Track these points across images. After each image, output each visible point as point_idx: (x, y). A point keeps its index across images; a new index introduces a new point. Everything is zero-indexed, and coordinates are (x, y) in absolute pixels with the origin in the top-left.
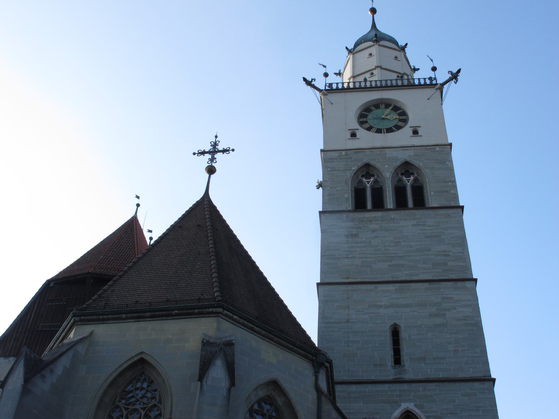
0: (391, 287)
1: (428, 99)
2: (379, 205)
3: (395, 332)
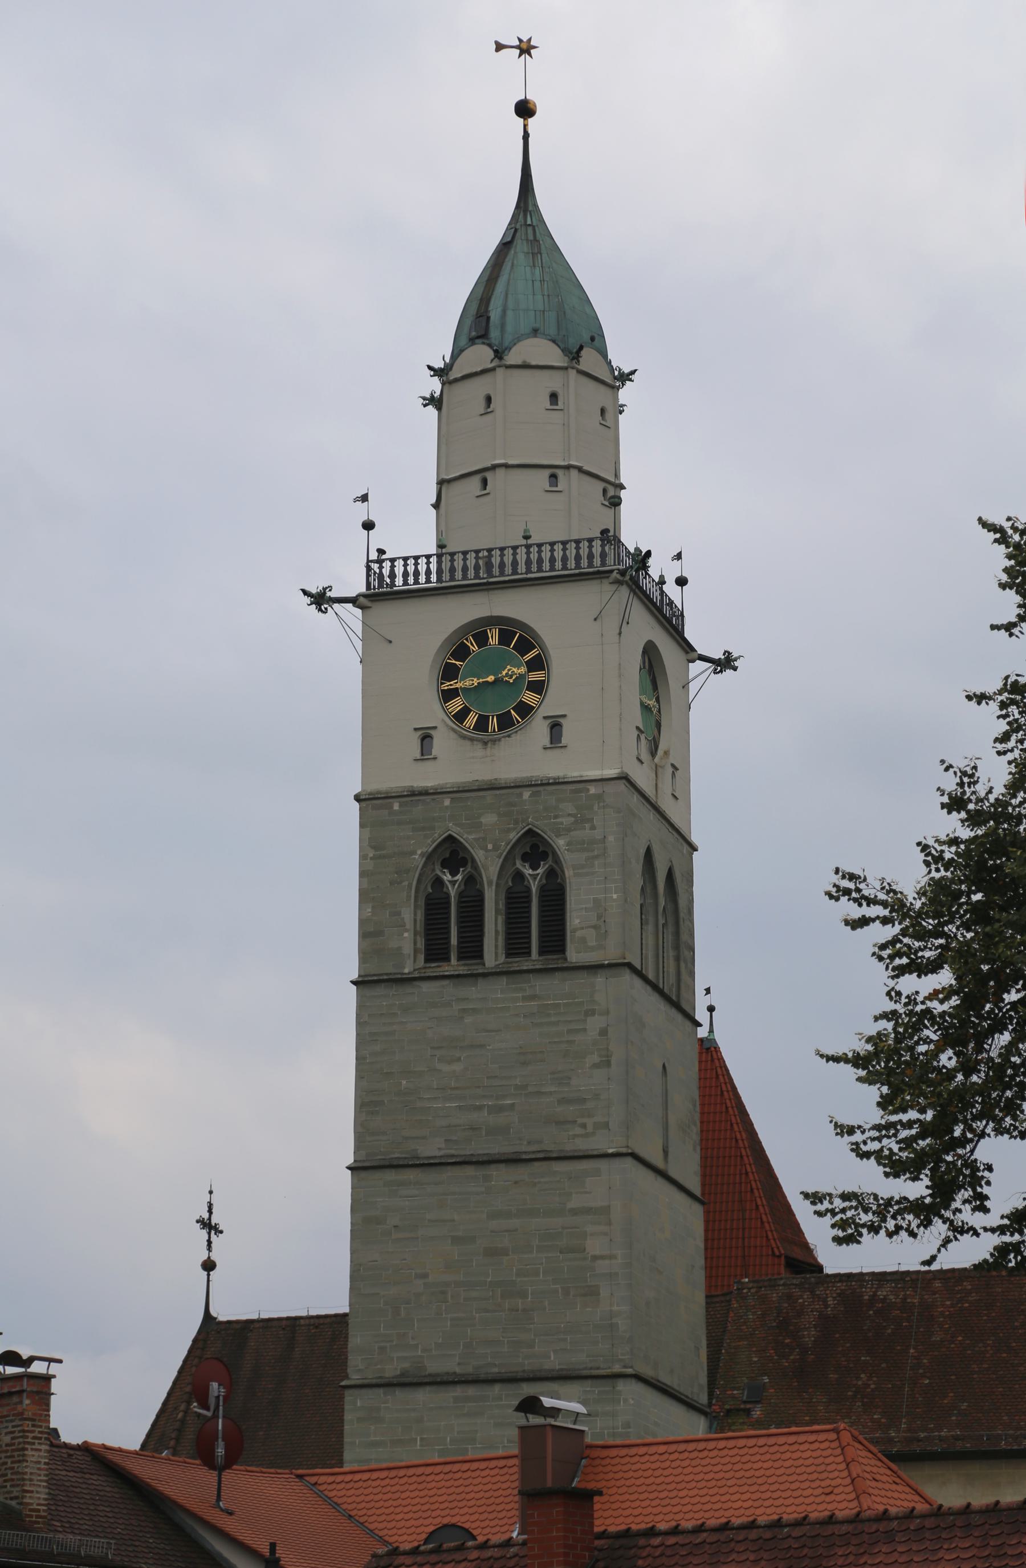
1: (595, 619)
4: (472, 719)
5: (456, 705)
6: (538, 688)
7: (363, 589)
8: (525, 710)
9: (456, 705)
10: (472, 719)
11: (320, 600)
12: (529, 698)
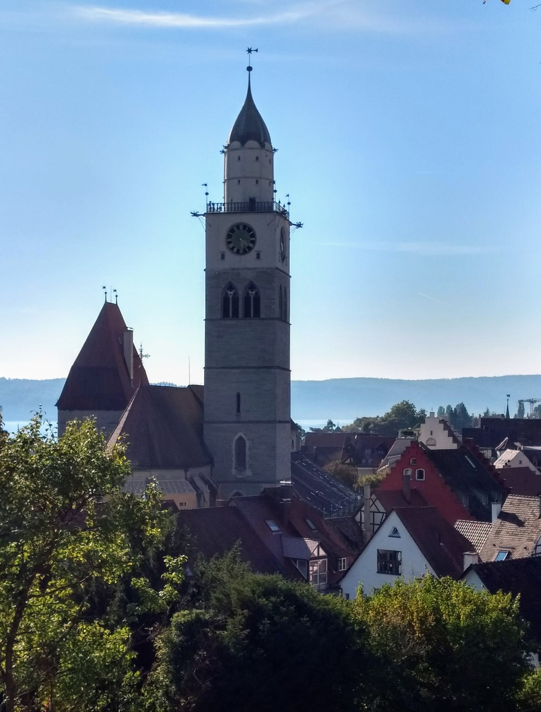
0: (237, 371)
2: (236, 315)
3: (238, 396)
4: (235, 250)
5: (231, 245)
6: (253, 242)
7: (206, 212)
8: (250, 249)
9: (231, 245)
10: (235, 250)
11: (195, 215)
12: (251, 245)
